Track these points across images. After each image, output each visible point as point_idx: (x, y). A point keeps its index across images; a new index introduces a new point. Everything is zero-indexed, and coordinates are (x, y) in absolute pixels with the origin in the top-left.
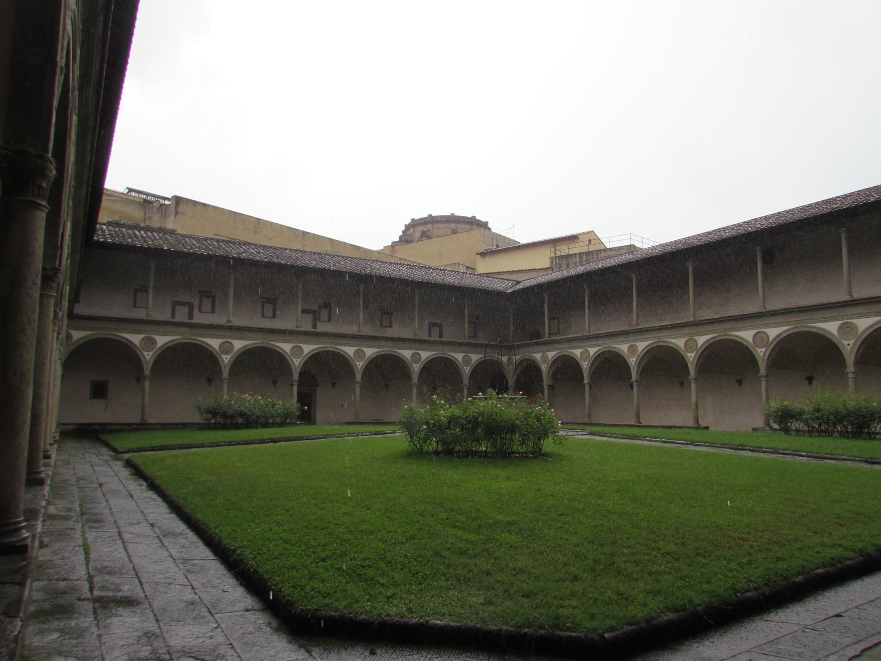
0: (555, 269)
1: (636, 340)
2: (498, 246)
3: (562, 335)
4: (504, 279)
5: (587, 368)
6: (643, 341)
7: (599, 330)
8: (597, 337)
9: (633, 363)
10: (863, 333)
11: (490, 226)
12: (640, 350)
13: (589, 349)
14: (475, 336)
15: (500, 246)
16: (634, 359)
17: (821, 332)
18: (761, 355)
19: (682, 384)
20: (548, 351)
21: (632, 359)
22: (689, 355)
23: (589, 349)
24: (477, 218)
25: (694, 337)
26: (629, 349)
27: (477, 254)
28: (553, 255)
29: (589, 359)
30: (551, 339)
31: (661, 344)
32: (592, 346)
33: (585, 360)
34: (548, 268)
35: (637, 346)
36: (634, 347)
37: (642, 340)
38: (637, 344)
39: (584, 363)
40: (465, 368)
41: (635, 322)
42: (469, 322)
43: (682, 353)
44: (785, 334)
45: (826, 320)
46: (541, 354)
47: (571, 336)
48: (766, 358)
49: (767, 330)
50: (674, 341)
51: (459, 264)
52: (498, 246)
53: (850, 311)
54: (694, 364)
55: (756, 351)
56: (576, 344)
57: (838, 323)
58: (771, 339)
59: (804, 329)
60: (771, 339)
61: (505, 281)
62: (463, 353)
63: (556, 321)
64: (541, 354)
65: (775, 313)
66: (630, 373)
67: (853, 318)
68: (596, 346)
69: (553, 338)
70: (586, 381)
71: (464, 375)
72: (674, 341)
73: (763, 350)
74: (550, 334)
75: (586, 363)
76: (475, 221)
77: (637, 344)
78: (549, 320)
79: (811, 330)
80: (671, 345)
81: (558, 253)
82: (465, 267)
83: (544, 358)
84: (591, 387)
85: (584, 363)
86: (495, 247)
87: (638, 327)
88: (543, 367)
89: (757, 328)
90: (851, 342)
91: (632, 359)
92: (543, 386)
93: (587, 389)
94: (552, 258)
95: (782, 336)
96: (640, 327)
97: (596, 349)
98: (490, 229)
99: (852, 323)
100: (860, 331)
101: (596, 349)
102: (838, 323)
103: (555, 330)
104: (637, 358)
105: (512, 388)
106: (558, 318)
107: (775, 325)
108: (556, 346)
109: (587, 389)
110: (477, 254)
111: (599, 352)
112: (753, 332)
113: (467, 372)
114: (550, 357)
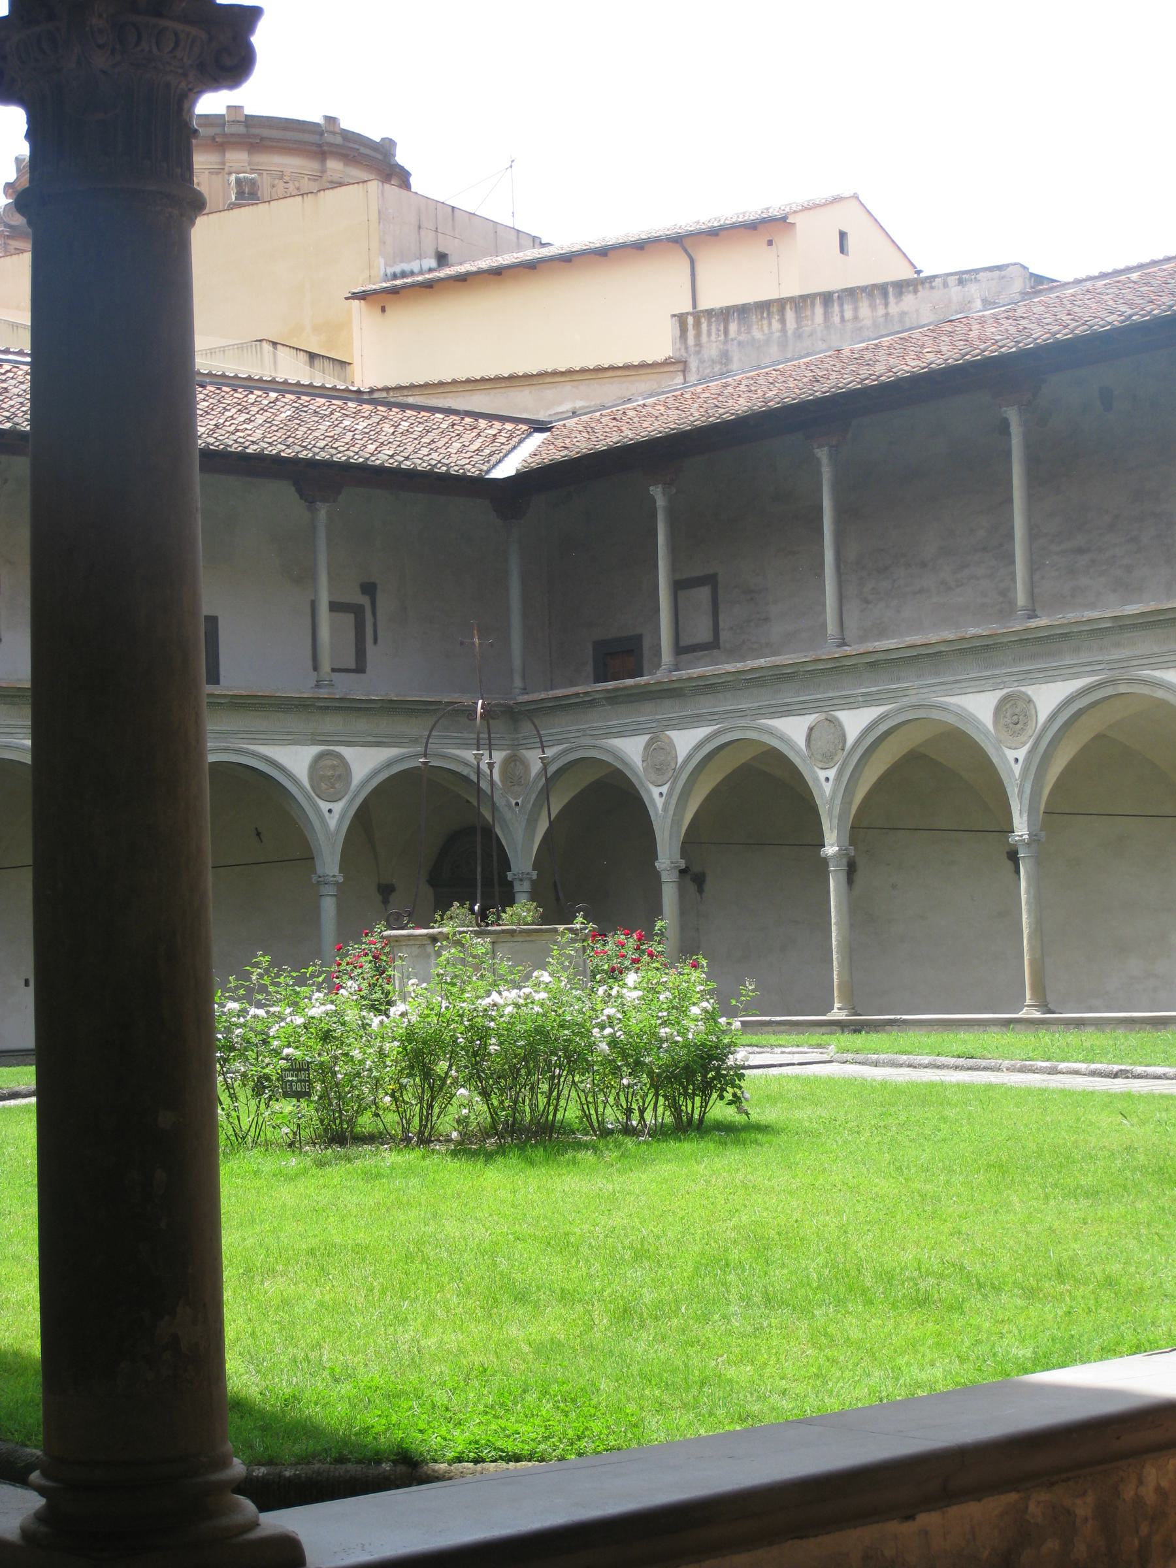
0: (693, 364)
1: (1028, 677)
2: (442, 259)
3: (735, 653)
4: (476, 416)
5: (834, 792)
6: (1052, 679)
7: (882, 632)
8: (879, 665)
9: (1017, 769)
11: (402, 158)
12: (1043, 715)
13: (843, 716)
14: (360, 668)
15: (451, 259)
16: (1021, 754)
20: (674, 727)
21: (1010, 754)
23: (843, 716)
24: (346, 124)
27: (356, 296)
28: (687, 307)
29: (840, 757)
30: (683, 674)
31: (1122, 689)
32: (852, 703)
33: (827, 760)
34: (667, 362)
35: (1030, 701)
36: (1021, 704)
37: (1052, 676)
38: (1030, 690)
39: (822, 774)
40: (324, 806)
41: (1021, 599)
42: (334, 607)
46: (647, 737)
47: (762, 662)
51: (275, 344)
52: (442, 259)
56: (788, 696)
61: (483, 423)
62: (314, 742)
63: (703, 594)
64: (647, 737)
68: (870, 700)
69: (694, 672)
70: (830, 849)
71: (321, 837)
74: (680, 650)
75: (832, 773)
76: (338, 140)
77: (1030, 690)
78: (679, 586)
80: (1159, 694)
81: (705, 304)
82: (303, 357)
83: (658, 751)
84: (851, 869)
85: (822, 774)
86: (433, 263)
87: (1033, 623)
88: (655, 791)
91: (1010, 754)
92: (657, 875)
93: (836, 884)
94: (681, 319)
96: (1043, 621)
97: (868, 715)
98: (401, 177)
101: (868, 715)
103: (703, 634)
104: (1032, 751)
105: (526, 886)
106: (710, 580)
108: (706, 704)
109: (836, 884)
110: (356, 296)
111: (883, 728)
113: (332, 822)
114: (682, 753)
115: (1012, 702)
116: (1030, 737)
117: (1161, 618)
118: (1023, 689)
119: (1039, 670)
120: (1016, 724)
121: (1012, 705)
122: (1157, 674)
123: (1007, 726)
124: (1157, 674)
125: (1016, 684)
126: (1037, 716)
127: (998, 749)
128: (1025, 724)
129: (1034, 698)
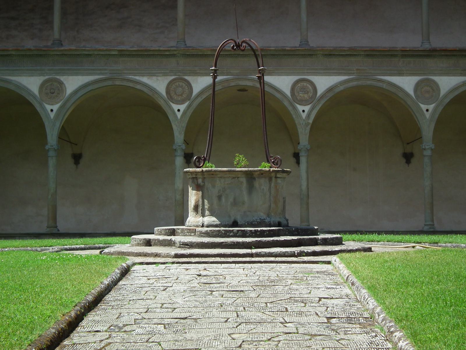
1: (64, 72)
10: (446, 96)
16: (55, 107)
17: (393, 90)
18: (304, 115)
19: (408, 157)
21: (48, 107)
22: (175, 107)
25: (186, 78)
26: (42, 86)
31: (118, 83)
38: (62, 78)
43: (162, 103)
44: (342, 88)
45: (400, 74)
48: (311, 121)
49: (315, 79)
50: (145, 80)
53: (429, 62)
54: (184, 125)
55: (295, 108)
57: (416, 79)
58: (319, 93)
59: (369, 83)
60: (319, 93)
65: (330, 54)
66: (44, 135)
67: (435, 75)
72: (145, 80)
73: (307, 108)
77: (62, 78)
79: (380, 84)
80: (138, 87)
89: (298, 74)
90: (431, 107)
91: (48, 107)
95: (337, 90)
99: (433, 81)
100: (443, 92)
102: (416, 79)
104: (61, 107)
107: (327, 71)
112: (293, 78)
115: (51, 83)
116: (62, 100)
117: (146, 53)
118: (58, 77)
119: (68, 70)
120: (53, 93)
121: (51, 84)
122: (137, 78)
123: (47, 94)
124: (137, 78)
125: (54, 75)
126: (66, 91)
127: (41, 105)
128: (59, 94)
129: (65, 82)
